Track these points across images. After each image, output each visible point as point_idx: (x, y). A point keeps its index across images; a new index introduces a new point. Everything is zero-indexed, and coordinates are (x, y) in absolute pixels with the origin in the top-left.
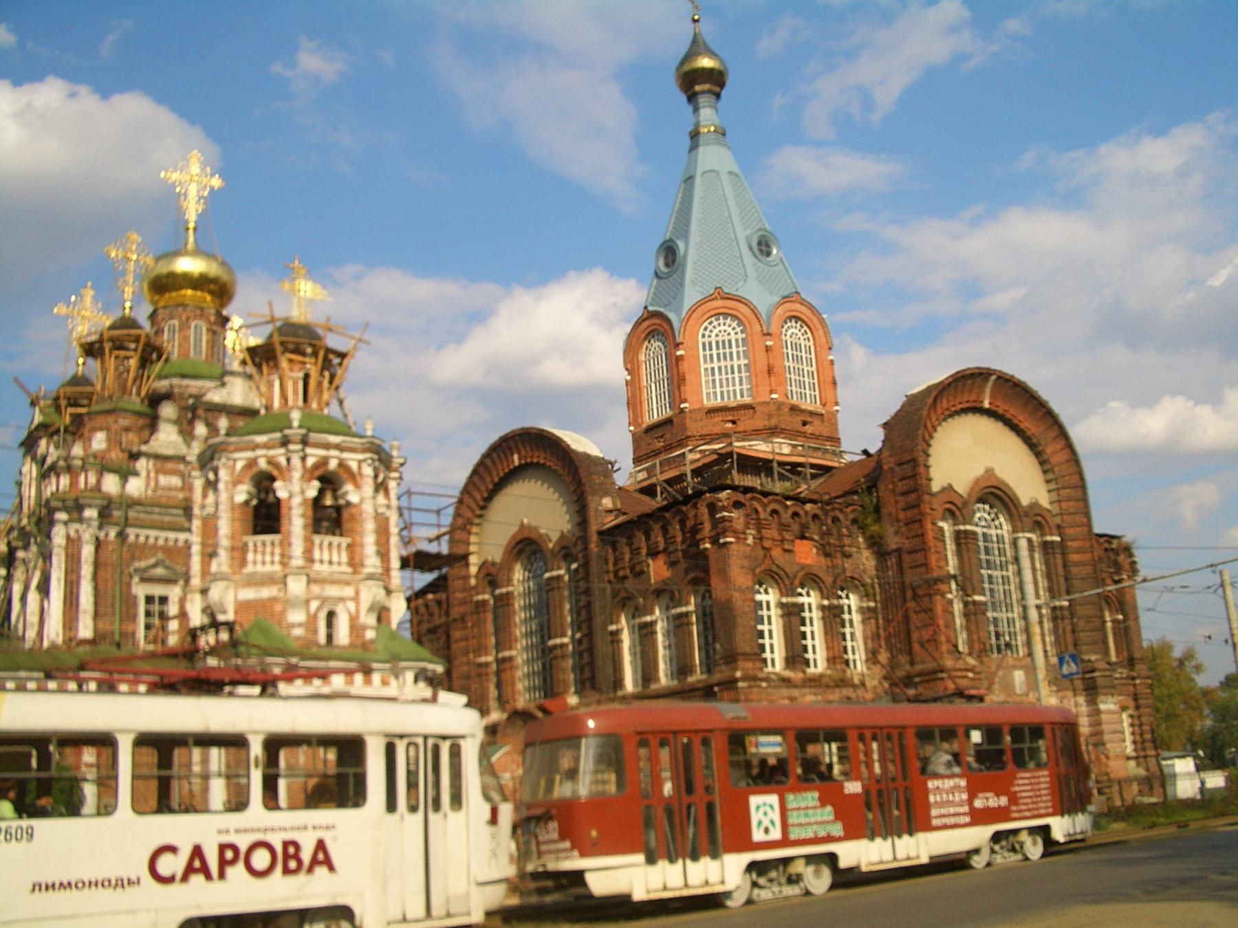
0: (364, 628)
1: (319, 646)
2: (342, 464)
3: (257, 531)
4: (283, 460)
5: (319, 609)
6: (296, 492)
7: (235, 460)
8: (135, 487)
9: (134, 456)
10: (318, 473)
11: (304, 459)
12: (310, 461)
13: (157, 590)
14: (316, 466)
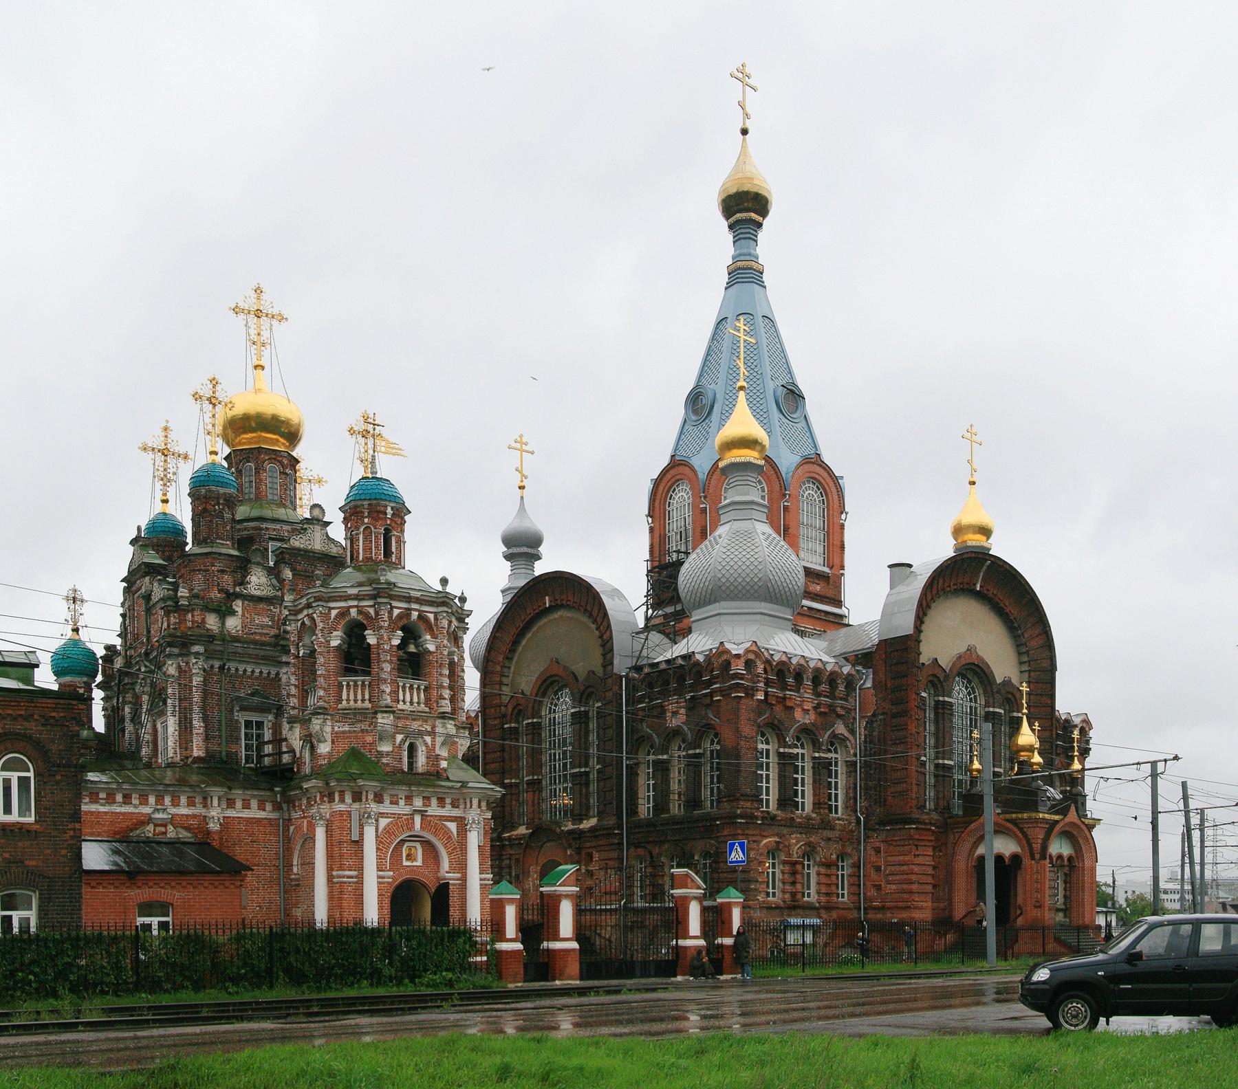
0: (438, 757)
1: (403, 772)
2: (422, 617)
3: (348, 671)
4: (372, 611)
5: (403, 741)
6: (384, 641)
7: (331, 609)
8: (233, 624)
9: (231, 596)
10: (401, 624)
11: (390, 613)
12: (396, 612)
13: (255, 717)
14: (400, 616)
